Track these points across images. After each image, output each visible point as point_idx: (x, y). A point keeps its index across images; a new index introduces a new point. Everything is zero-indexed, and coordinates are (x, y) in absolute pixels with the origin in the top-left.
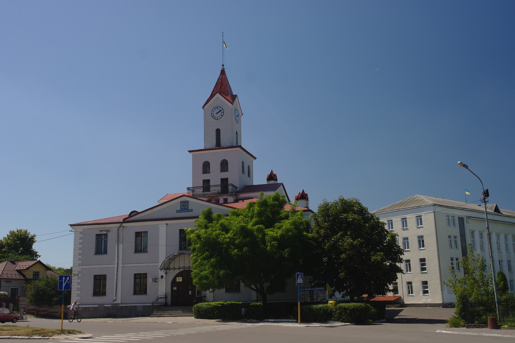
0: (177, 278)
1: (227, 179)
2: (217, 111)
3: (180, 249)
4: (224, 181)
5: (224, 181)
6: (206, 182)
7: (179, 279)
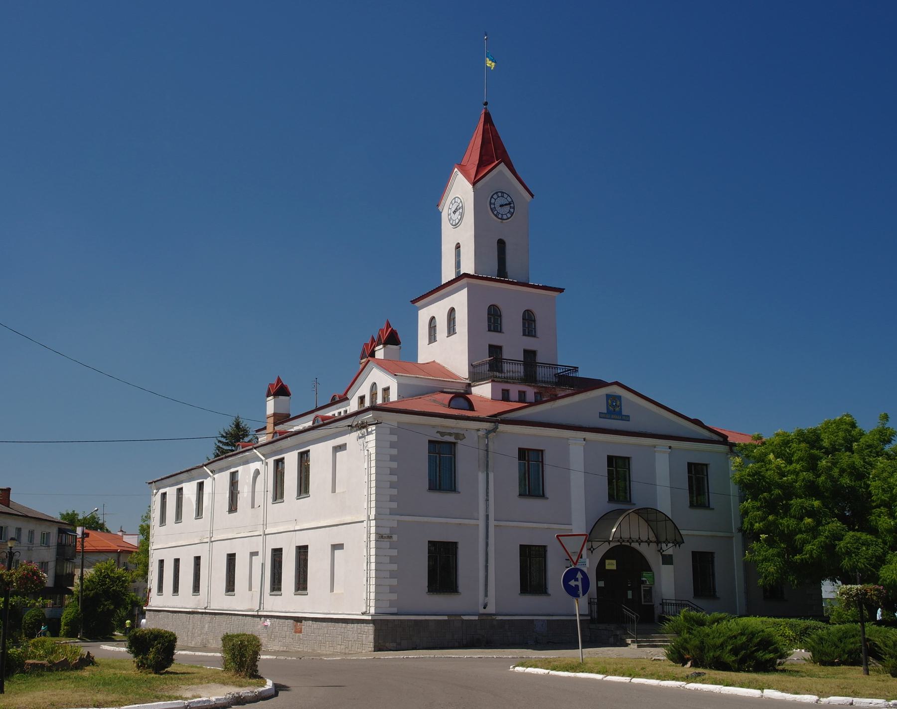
0: (607, 561)
2: (504, 201)
3: (611, 498)
4: (530, 355)
5: (530, 355)
6: (495, 350)
7: (611, 565)
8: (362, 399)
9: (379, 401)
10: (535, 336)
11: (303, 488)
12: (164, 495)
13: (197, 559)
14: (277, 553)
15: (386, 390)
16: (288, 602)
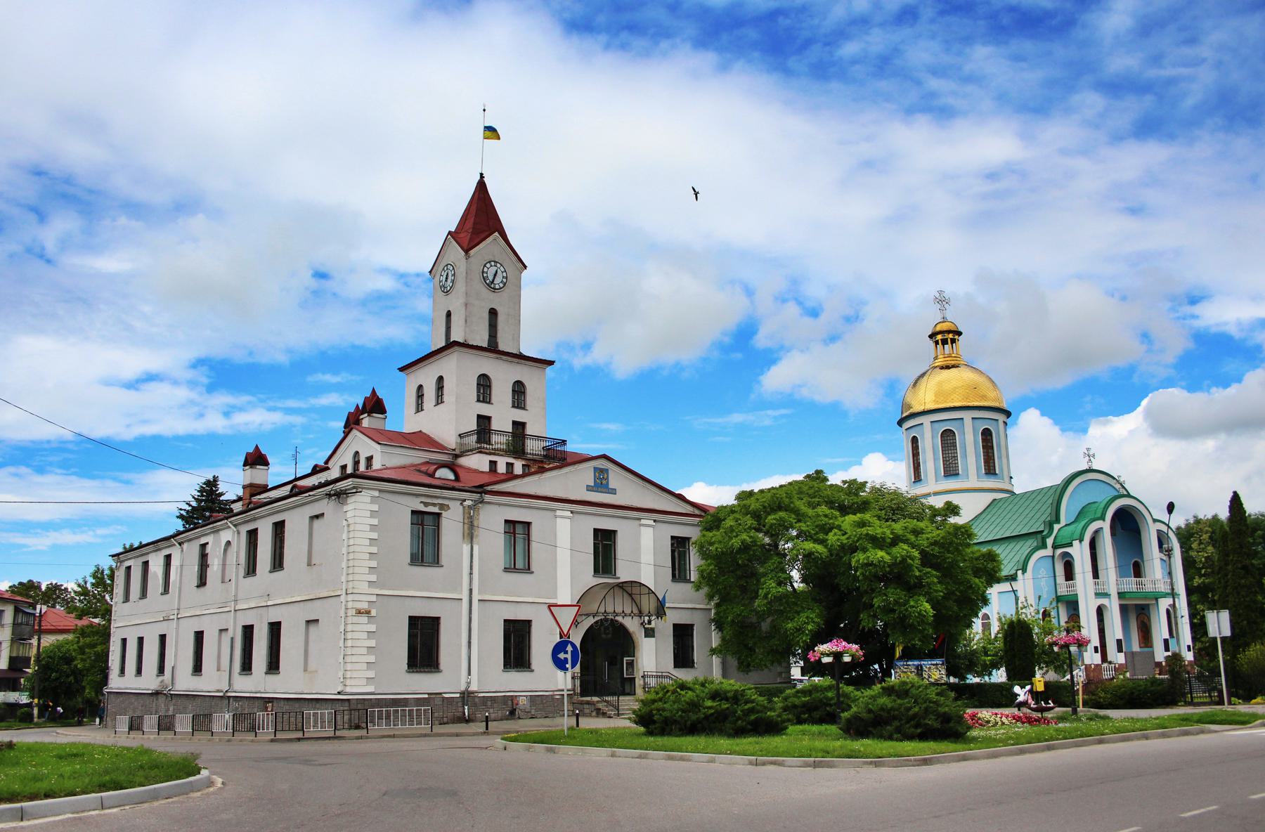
1: (523, 425)
4: (519, 426)
5: (519, 426)
6: (484, 421)
8: (344, 467)
9: (362, 467)
10: (524, 408)
11: (278, 562)
12: (129, 568)
13: (163, 638)
14: (248, 631)
15: (369, 459)
16: (258, 683)
